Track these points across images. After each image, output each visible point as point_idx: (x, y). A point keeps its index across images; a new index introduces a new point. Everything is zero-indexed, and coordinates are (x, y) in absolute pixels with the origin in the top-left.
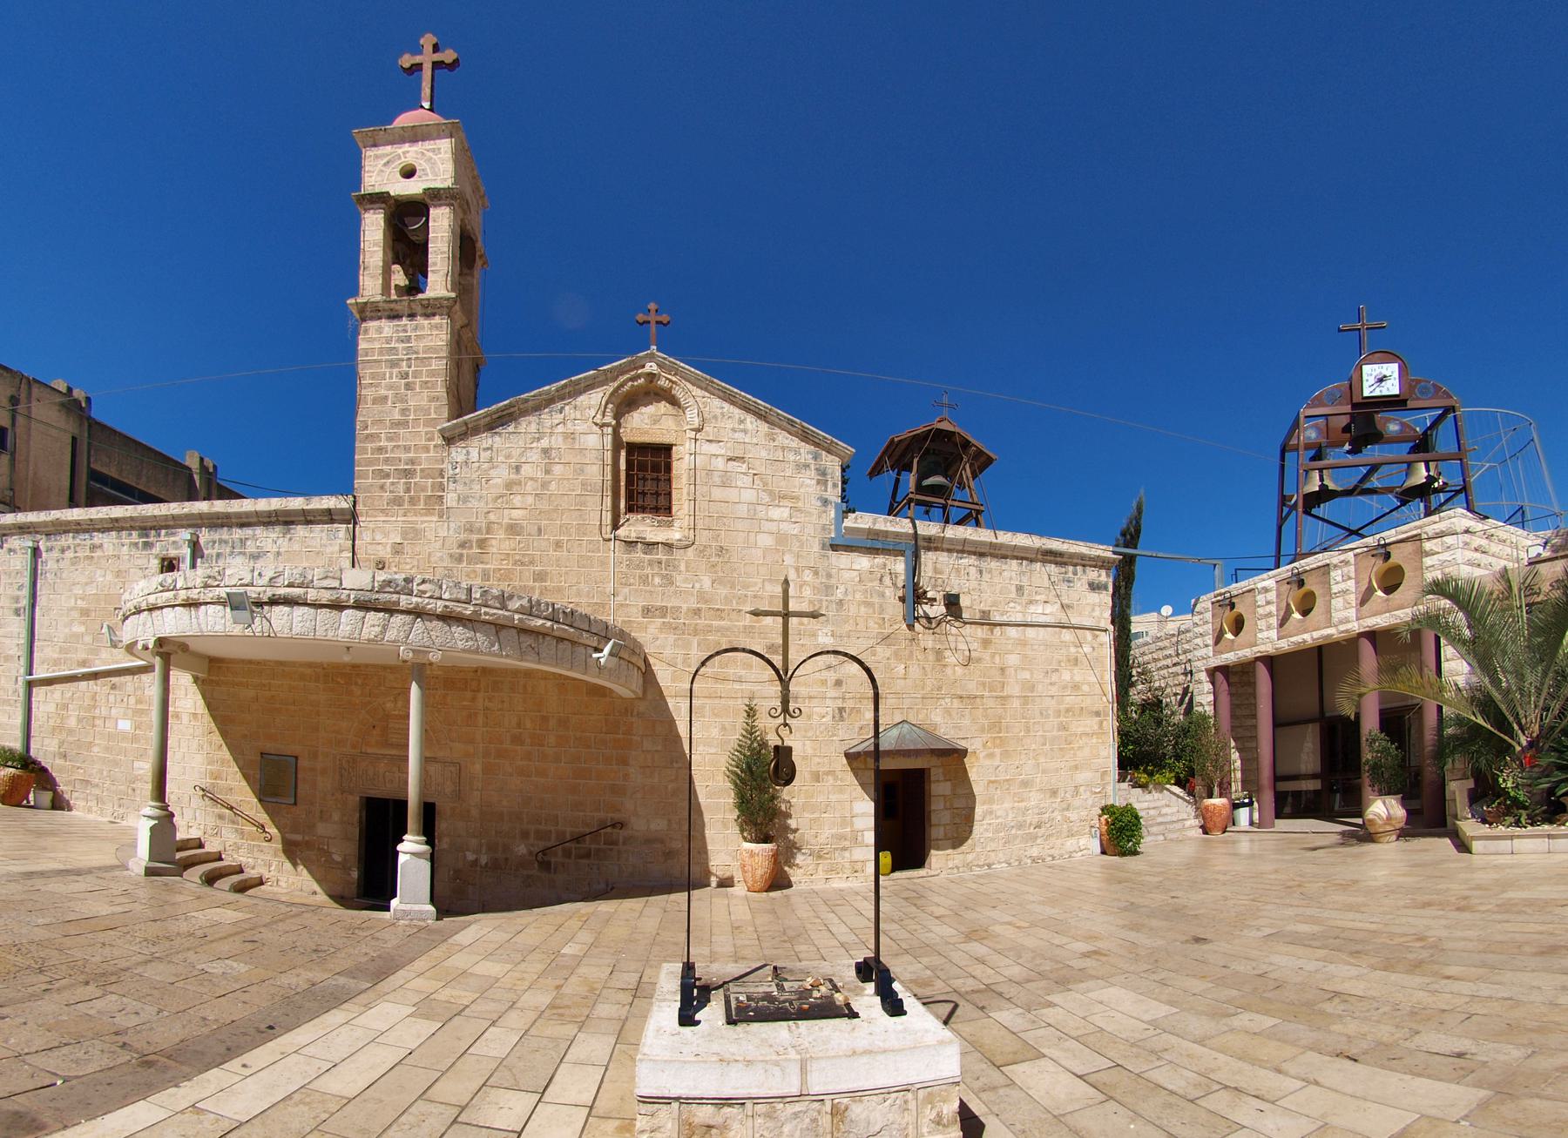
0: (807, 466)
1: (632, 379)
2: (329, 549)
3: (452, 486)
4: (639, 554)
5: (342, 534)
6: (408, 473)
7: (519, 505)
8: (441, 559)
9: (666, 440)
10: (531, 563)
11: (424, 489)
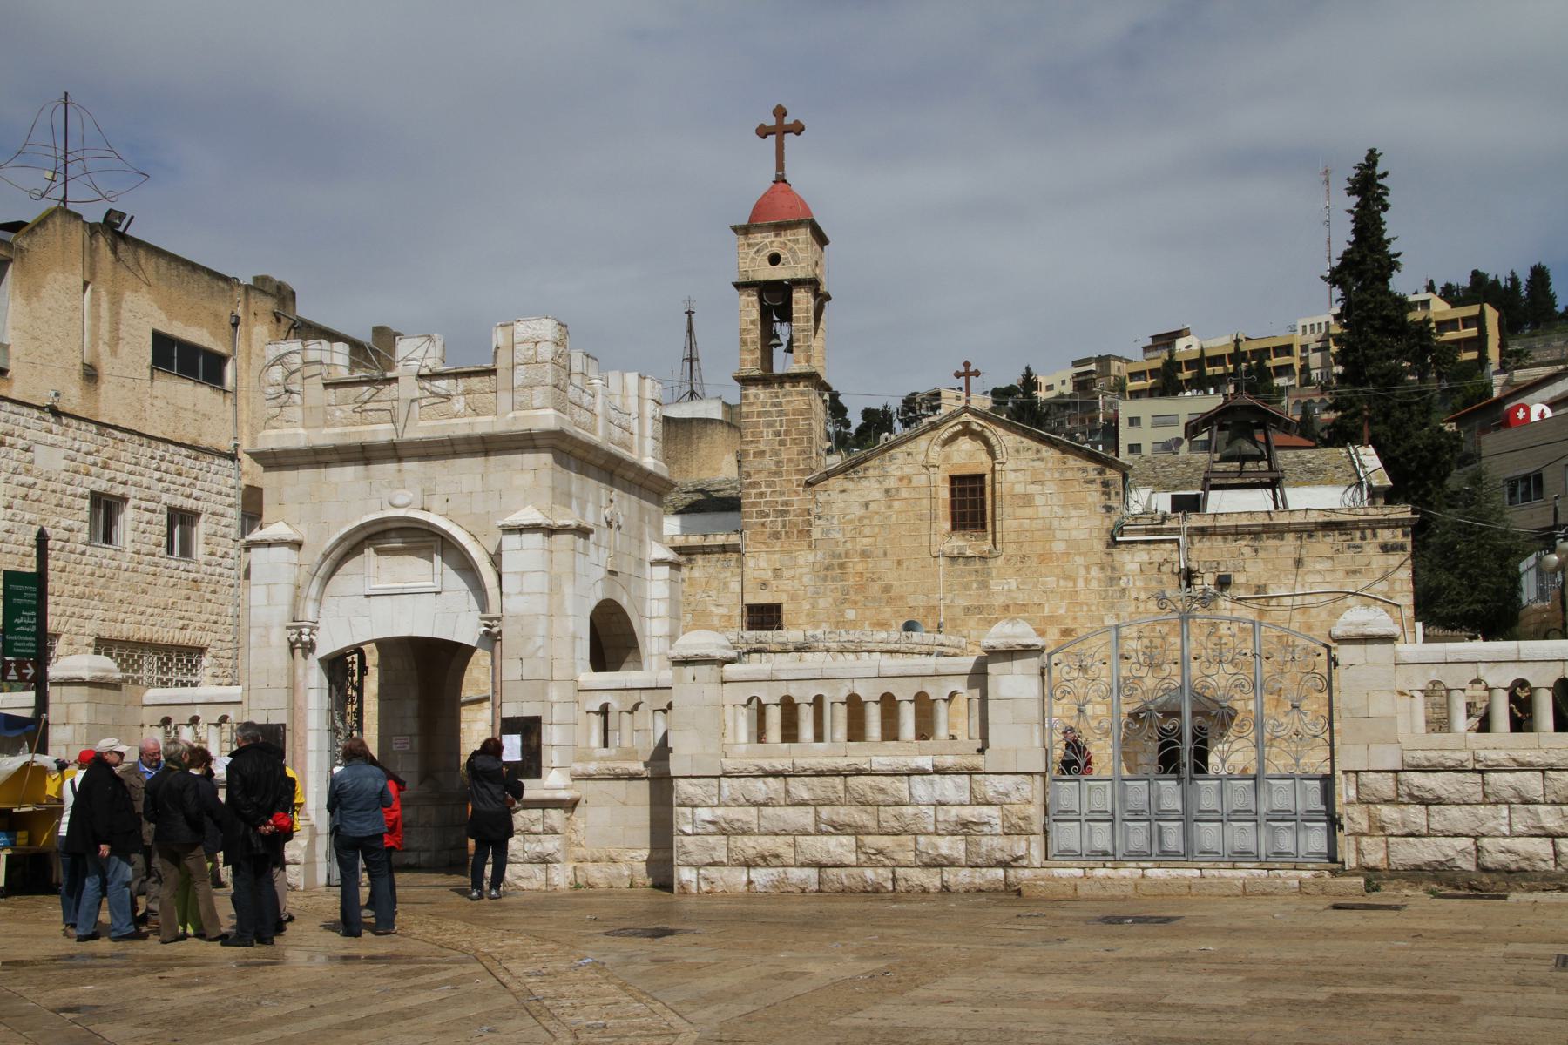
0: (1092, 481)
1: (951, 427)
2: (722, 576)
3: (818, 522)
4: (960, 566)
5: (732, 564)
6: (784, 513)
7: (868, 534)
8: (811, 579)
9: (980, 471)
10: (879, 579)
11: (796, 525)
